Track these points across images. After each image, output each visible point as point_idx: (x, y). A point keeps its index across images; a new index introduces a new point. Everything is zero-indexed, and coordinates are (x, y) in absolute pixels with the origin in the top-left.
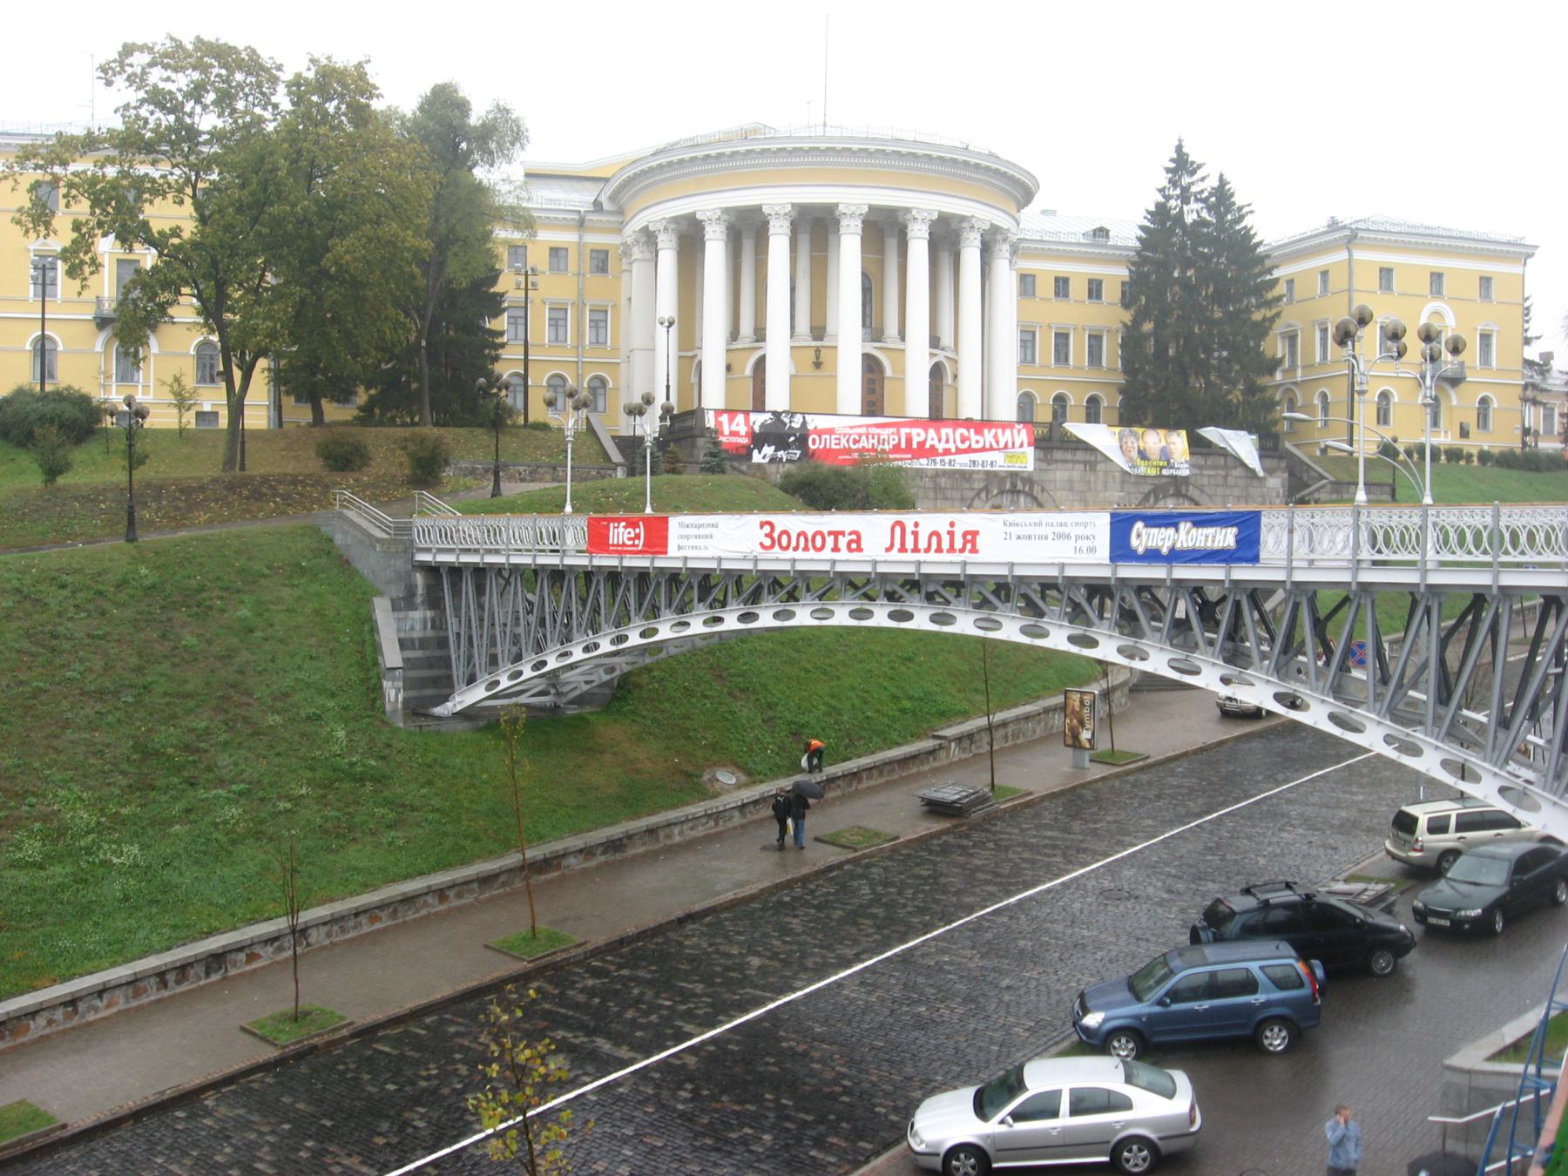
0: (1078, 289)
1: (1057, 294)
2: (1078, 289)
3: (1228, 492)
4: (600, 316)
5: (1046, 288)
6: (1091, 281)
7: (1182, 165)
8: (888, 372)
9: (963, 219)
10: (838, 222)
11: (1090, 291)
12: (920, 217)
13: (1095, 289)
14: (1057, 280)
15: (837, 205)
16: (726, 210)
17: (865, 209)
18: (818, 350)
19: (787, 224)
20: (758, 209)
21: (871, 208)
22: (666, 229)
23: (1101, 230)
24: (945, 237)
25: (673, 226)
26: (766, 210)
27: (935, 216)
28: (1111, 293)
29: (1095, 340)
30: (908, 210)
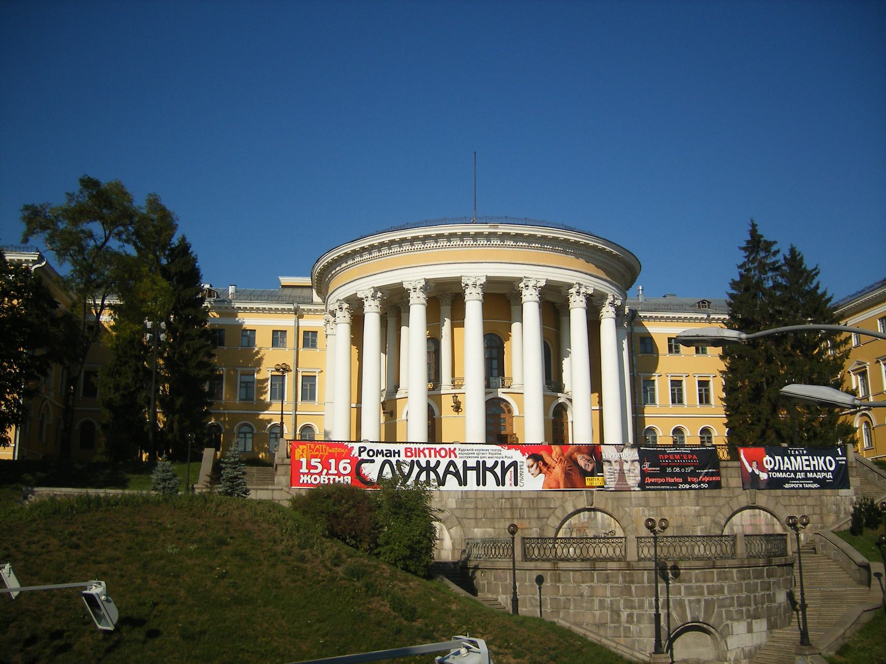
3: (803, 501)
7: (756, 244)
8: (516, 412)
9: (571, 286)
12: (531, 284)
17: (483, 280)
18: (455, 396)
20: (401, 283)
23: (703, 302)
25: (345, 306)
26: (406, 286)
27: (543, 283)
29: (704, 384)
30: (520, 280)
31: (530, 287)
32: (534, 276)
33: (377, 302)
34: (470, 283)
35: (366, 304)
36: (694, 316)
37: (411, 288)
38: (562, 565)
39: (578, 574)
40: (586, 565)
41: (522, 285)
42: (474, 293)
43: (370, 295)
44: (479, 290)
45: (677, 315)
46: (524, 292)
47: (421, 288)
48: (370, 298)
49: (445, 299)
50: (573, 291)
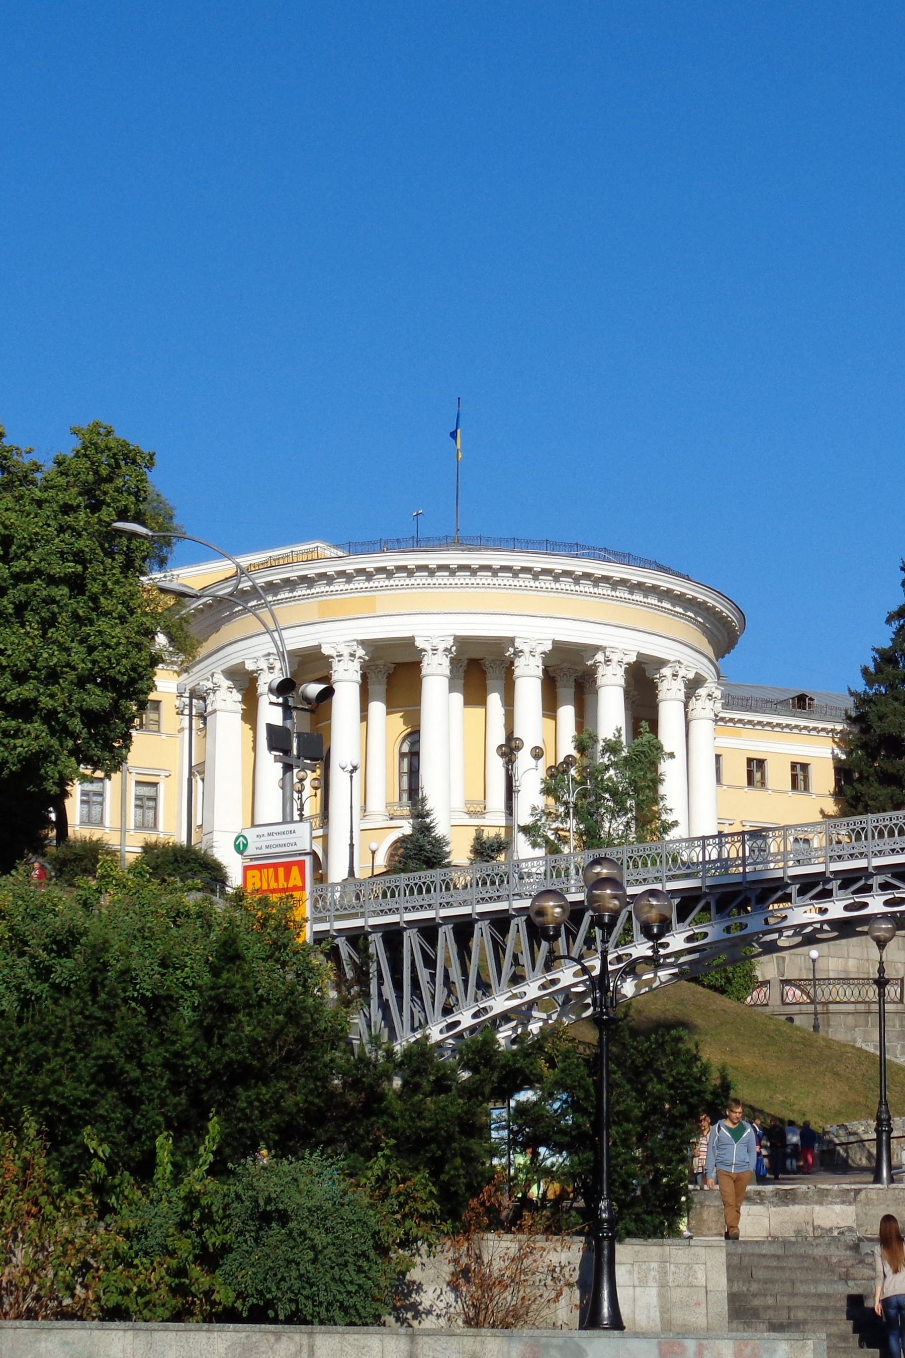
0: (778, 775)
1: (750, 782)
2: (778, 775)
4: (146, 791)
5: (737, 772)
6: (794, 766)
9: (662, 663)
10: (512, 663)
11: (794, 778)
12: (615, 658)
13: (800, 774)
14: (750, 761)
15: (512, 640)
16: (363, 643)
17: (548, 647)
19: (446, 662)
21: (555, 642)
22: (271, 668)
24: (642, 683)
26: (420, 643)
27: (632, 658)
28: (824, 779)
30: (598, 648)
31: (614, 663)
32: (621, 646)
33: (356, 665)
34: (526, 649)
35: (336, 666)
36: (793, 721)
37: (428, 647)
38: (832, 1007)
39: (850, 1017)
40: (861, 1007)
41: (600, 657)
42: (532, 666)
43: (346, 652)
44: (539, 662)
45: (765, 718)
46: (601, 670)
47: (446, 650)
48: (346, 657)
49: (481, 668)
50: (666, 671)
